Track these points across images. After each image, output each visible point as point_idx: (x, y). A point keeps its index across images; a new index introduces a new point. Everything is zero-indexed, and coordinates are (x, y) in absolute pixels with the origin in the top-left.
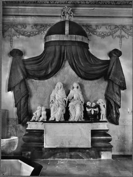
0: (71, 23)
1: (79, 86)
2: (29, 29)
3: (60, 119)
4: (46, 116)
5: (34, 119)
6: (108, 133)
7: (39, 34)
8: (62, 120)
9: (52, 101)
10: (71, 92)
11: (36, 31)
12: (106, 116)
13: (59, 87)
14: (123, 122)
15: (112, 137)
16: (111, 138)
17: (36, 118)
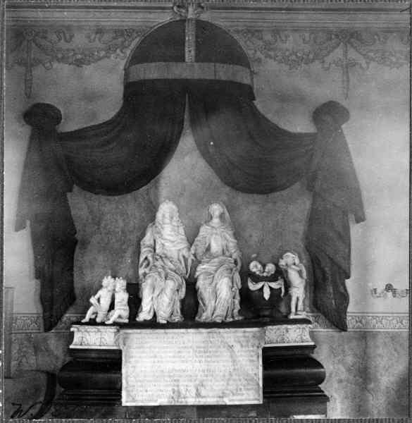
0: (201, 26)
1: (227, 214)
2: (79, 40)
3: (171, 317)
4: (128, 308)
5: (93, 317)
6: (314, 356)
7: (109, 57)
8: (177, 320)
9: (146, 258)
10: (204, 230)
11: (102, 50)
12: (307, 303)
13: (167, 215)
14: (361, 322)
15: (329, 366)
16: (324, 373)
17: (97, 313)
